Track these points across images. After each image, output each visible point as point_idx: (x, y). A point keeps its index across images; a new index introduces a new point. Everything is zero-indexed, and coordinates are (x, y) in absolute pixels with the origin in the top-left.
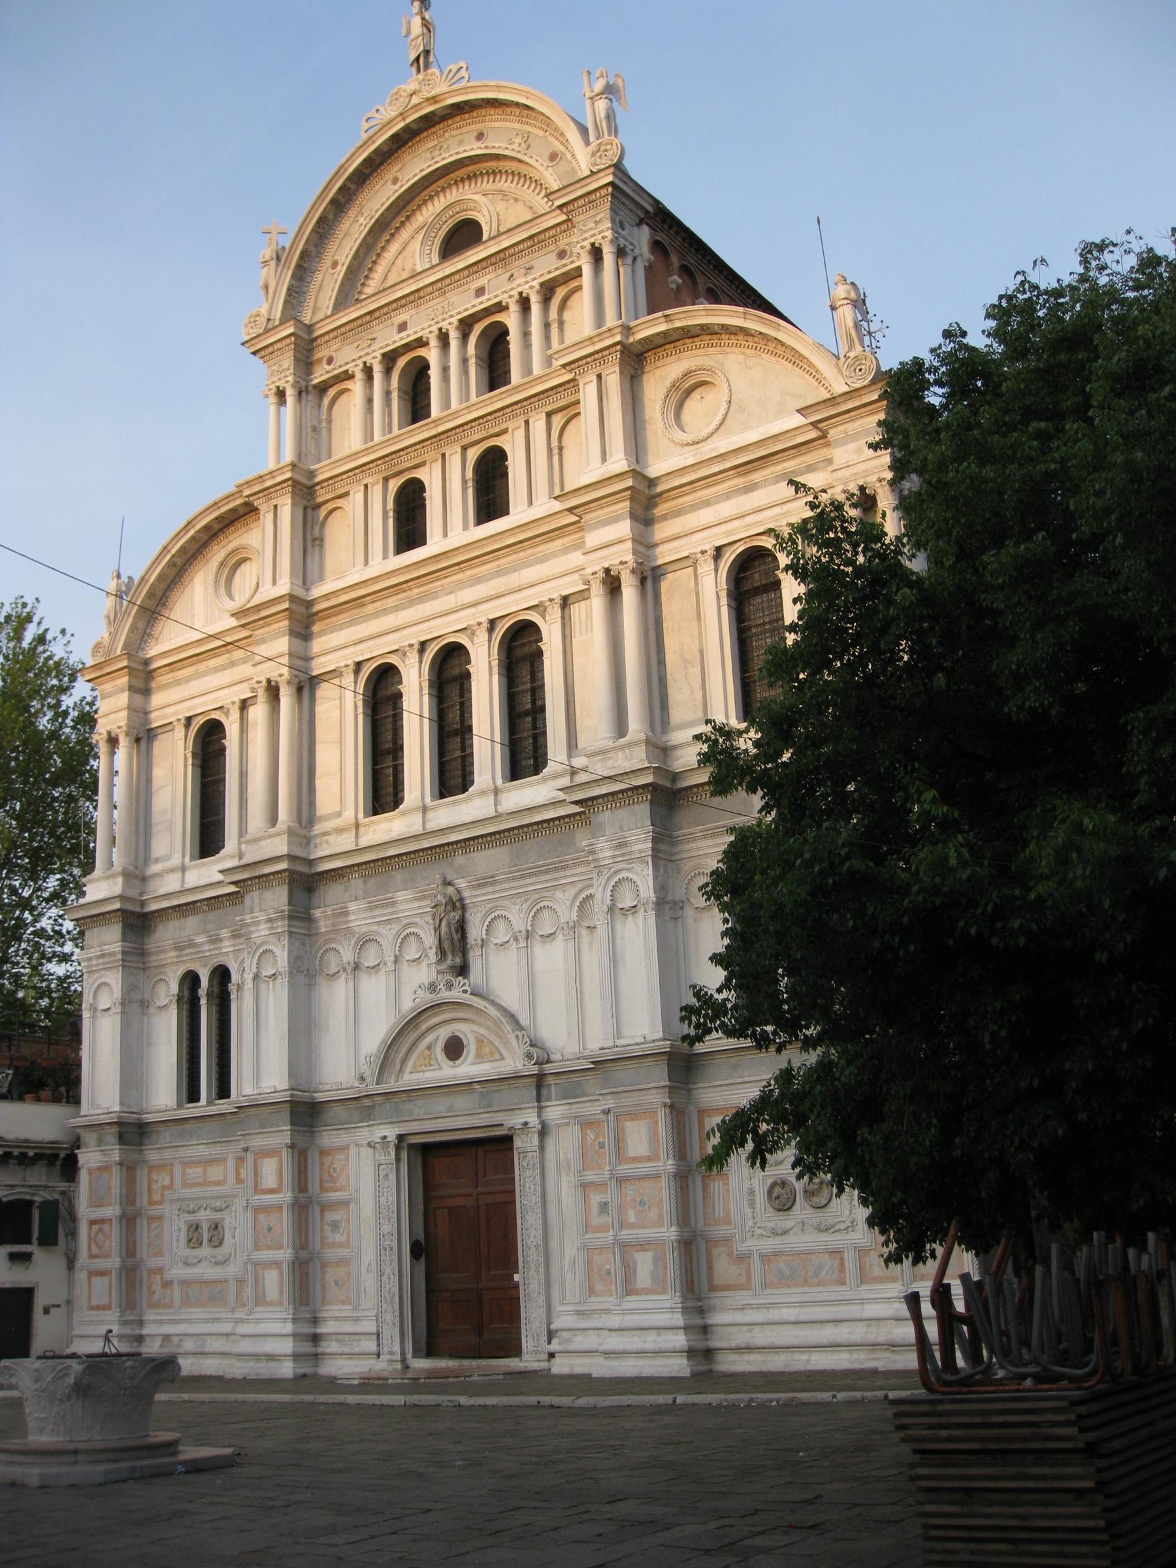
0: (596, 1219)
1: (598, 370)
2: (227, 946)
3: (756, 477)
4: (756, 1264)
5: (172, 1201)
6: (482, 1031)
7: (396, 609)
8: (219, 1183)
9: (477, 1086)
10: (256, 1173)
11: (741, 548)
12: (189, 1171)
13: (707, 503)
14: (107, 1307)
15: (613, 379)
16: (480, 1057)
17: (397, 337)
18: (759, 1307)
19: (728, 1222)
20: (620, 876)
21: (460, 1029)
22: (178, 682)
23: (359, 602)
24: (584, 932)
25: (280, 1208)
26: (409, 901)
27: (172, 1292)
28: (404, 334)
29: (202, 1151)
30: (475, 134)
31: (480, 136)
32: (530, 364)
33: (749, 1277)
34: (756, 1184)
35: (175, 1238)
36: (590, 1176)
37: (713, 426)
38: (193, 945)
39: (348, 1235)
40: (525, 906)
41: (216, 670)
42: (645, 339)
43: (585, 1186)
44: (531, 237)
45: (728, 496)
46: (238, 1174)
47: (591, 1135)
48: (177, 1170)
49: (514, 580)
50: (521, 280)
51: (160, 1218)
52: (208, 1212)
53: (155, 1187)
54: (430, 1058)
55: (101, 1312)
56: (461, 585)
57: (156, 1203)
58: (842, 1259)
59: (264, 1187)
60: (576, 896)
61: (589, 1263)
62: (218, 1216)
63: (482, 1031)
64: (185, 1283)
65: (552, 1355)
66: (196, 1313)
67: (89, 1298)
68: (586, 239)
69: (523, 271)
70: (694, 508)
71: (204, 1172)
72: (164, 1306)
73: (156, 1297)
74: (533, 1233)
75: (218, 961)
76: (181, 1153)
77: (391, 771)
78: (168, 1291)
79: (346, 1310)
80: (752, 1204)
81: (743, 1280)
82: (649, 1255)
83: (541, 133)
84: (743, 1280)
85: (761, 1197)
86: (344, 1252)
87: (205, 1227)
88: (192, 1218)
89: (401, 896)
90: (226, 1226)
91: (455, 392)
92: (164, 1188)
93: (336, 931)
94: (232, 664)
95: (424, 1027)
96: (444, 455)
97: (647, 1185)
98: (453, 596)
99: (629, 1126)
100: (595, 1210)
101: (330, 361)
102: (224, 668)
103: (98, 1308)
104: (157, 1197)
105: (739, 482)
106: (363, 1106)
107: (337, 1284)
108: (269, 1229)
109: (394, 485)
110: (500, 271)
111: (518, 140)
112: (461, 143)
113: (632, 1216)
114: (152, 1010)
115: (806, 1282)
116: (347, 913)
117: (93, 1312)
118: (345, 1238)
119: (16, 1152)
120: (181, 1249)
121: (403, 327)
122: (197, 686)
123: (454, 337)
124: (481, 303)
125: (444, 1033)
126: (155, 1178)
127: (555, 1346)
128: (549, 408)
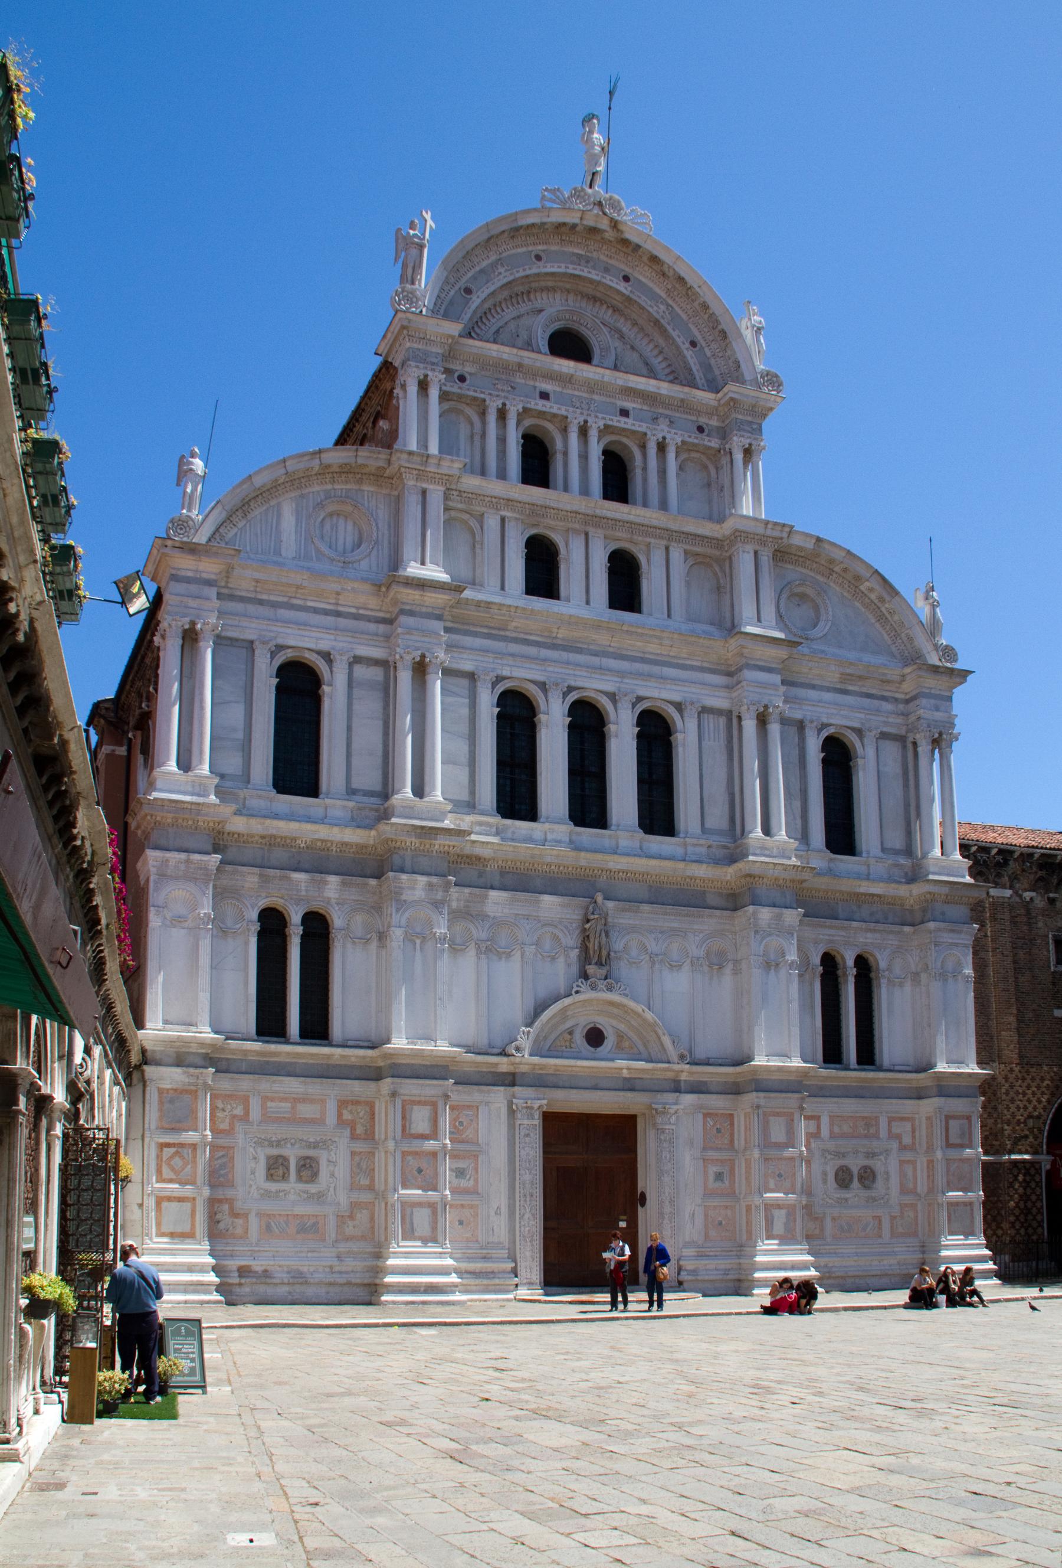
0: (712, 1184)
1: (757, 548)
8: (312, 1122)
10: (404, 1118)
12: (269, 1104)
25: (434, 1154)
30: (623, 274)
31: (626, 279)
33: (822, 1230)
39: (476, 1181)
44: (682, 400)
46: (340, 1115)
50: (666, 429)
53: (220, 1114)
54: (571, 1041)
58: (880, 1221)
59: (413, 1131)
61: (706, 1216)
63: (622, 1027)
68: (743, 436)
71: (293, 1108)
73: (221, 1226)
75: (315, 906)
80: (825, 1181)
81: (817, 1232)
82: (783, 1212)
84: (817, 1232)
85: (831, 1177)
88: (275, 1152)
92: (234, 1116)
96: (587, 534)
100: (711, 1178)
104: (225, 1126)
108: (420, 1171)
110: (645, 408)
111: (662, 307)
112: (607, 270)
116: (486, 897)
118: (472, 1182)
121: (544, 396)
123: (593, 434)
124: (625, 423)
126: (220, 1105)
128: (688, 547)
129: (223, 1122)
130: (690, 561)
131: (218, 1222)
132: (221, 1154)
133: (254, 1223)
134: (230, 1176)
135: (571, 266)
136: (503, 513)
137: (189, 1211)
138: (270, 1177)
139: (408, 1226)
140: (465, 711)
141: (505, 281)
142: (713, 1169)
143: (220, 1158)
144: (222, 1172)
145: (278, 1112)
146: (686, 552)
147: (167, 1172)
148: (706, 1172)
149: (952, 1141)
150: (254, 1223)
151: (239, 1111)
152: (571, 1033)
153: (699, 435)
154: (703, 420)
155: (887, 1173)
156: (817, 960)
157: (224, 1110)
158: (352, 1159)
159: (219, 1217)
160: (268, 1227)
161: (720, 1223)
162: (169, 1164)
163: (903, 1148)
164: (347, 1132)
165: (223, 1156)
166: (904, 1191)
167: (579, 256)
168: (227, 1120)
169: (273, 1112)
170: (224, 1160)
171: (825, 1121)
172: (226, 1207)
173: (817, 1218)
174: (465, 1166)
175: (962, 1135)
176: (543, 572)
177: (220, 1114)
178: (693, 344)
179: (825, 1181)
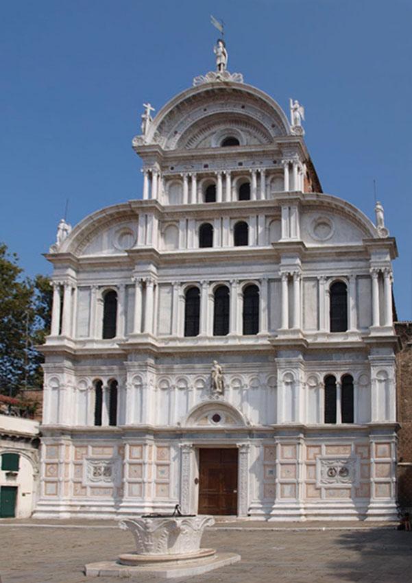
0: (267, 475)
2: (116, 372)
3: (342, 258)
4: (323, 491)
5: (87, 459)
6: (228, 414)
7: (198, 267)
9: (227, 432)
11: (334, 279)
13: (324, 261)
15: (295, 212)
16: (227, 421)
17: (203, 169)
18: (322, 503)
19: (315, 478)
20: (288, 372)
21: (220, 413)
22: (95, 271)
23: (183, 261)
24: (268, 388)
26: (200, 368)
27: (86, 491)
28: (206, 169)
29: (104, 444)
31: (243, 107)
32: (260, 194)
34: (323, 469)
36: (266, 463)
37: (328, 237)
38: (100, 370)
39: (169, 475)
40: (247, 377)
41: (113, 271)
42: (308, 201)
43: (265, 465)
44: (264, 151)
45: (332, 261)
47: (267, 450)
48: (90, 448)
49: (249, 268)
51: (81, 464)
53: (78, 453)
56: (227, 265)
57: (79, 459)
60: (266, 377)
64: (91, 487)
65: (249, 515)
66: (98, 498)
69: (259, 162)
70: (319, 262)
72: (81, 495)
73: (78, 492)
74: (244, 478)
75: (111, 377)
77: (192, 323)
78: (84, 490)
79: (166, 499)
83: (269, 115)
84: (318, 495)
86: (167, 480)
89: (198, 366)
90: (113, 469)
91: (227, 194)
93: (168, 374)
94: (122, 270)
95: (205, 410)
96: (222, 218)
97: (290, 466)
98: (224, 268)
99: (285, 448)
100: (267, 473)
101: (172, 168)
102: (117, 271)
104: (79, 457)
105: (337, 258)
106: (177, 434)
107: (162, 490)
109: (199, 224)
111: (259, 114)
113: (284, 475)
114: (77, 390)
115: (338, 496)
118: (167, 476)
119: (10, 435)
120: (91, 476)
121: (206, 166)
122: (103, 275)
125: (213, 413)
127: (251, 512)
128: (266, 214)
130: (269, 220)
133: (89, 490)
135: (219, 109)
136: (187, 218)
140: (170, 298)
141: (192, 124)
142: (268, 469)
146: (266, 216)
147: (49, 474)
148: (265, 470)
149: (378, 455)
150: (89, 490)
151: (84, 452)
152: (206, 417)
153: (274, 165)
154: (276, 158)
155: (354, 470)
156: (321, 380)
161: (271, 491)
163: (363, 458)
164: (121, 459)
166: (362, 476)
167: (223, 104)
171: (324, 448)
173: (317, 489)
175: (384, 452)
176: (206, 237)
178: (273, 126)
179: (322, 474)
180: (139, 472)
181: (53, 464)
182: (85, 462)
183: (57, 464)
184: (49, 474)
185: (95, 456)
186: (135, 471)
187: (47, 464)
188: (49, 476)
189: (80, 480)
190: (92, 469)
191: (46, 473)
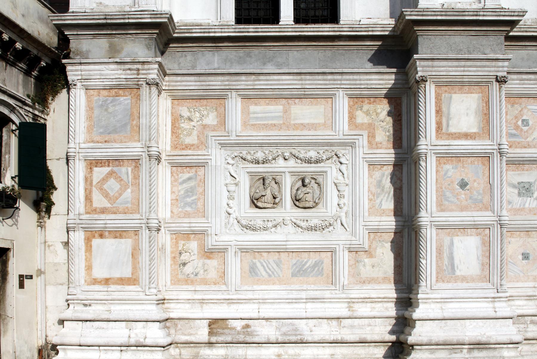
5: (223, 145)
12: (253, 108)
14: (132, 281)
35: (226, 194)
48: (235, 106)
51: (203, 165)
52: (292, 162)
55: (113, 287)
62: (312, 168)
67: (89, 268)
71: (285, 112)
76: (243, 83)
78: (213, 263)
87: (288, 182)
88: (260, 169)
92: (205, 126)
103: (107, 281)
117: (97, 287)
120: (243, 209)
126: (185, 113)
129: (189, 134)
131: (184, 264)
132: (186, 176)
133: (235, 265)
134: (200, 204)
137: (129, 250)
138: (255, 202)
139: (446, 261)
143: (184, 181)
144: (189, 200)
145: (266, 118)
150: (235, 265)
151: (211, 119)
157: (190, 119)
158: (370, 176)
159: (185, 257)
160: (253, 270)
162: (101, 189)
165: (190, 179)
168: (195, 133)
169: (257, 118)
170: (192, 183)
172: (193, 245)
174: (532, 180)
177: (185, 125)
180: (478, 184)
181: (118, 161)
182: (217, 157)
183: (136, 161)
184: (99, 200)
185: (258, 136)
186: (463, 185)
187: (93, 163)
188: (103, 211)
189: (198, 223)
190: (245, 182)
191: (88, 198)
